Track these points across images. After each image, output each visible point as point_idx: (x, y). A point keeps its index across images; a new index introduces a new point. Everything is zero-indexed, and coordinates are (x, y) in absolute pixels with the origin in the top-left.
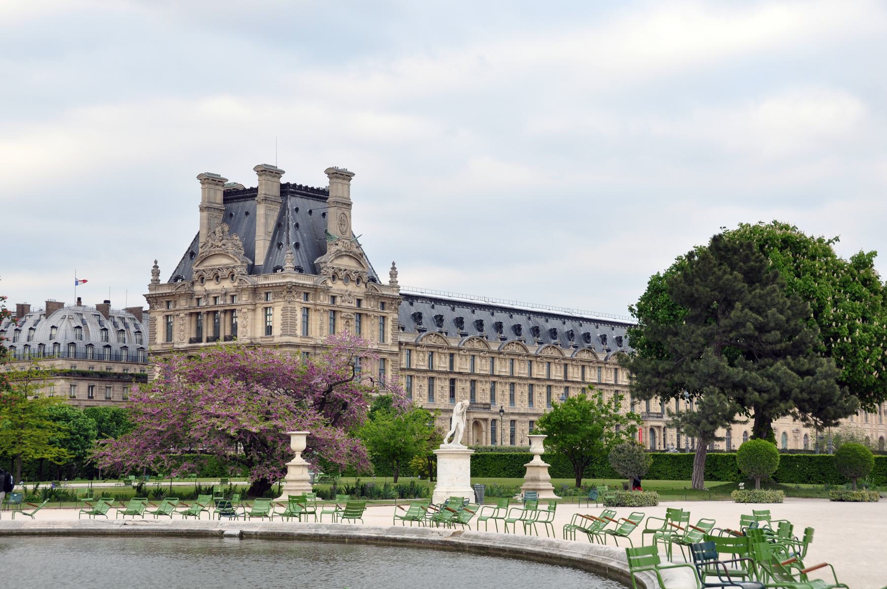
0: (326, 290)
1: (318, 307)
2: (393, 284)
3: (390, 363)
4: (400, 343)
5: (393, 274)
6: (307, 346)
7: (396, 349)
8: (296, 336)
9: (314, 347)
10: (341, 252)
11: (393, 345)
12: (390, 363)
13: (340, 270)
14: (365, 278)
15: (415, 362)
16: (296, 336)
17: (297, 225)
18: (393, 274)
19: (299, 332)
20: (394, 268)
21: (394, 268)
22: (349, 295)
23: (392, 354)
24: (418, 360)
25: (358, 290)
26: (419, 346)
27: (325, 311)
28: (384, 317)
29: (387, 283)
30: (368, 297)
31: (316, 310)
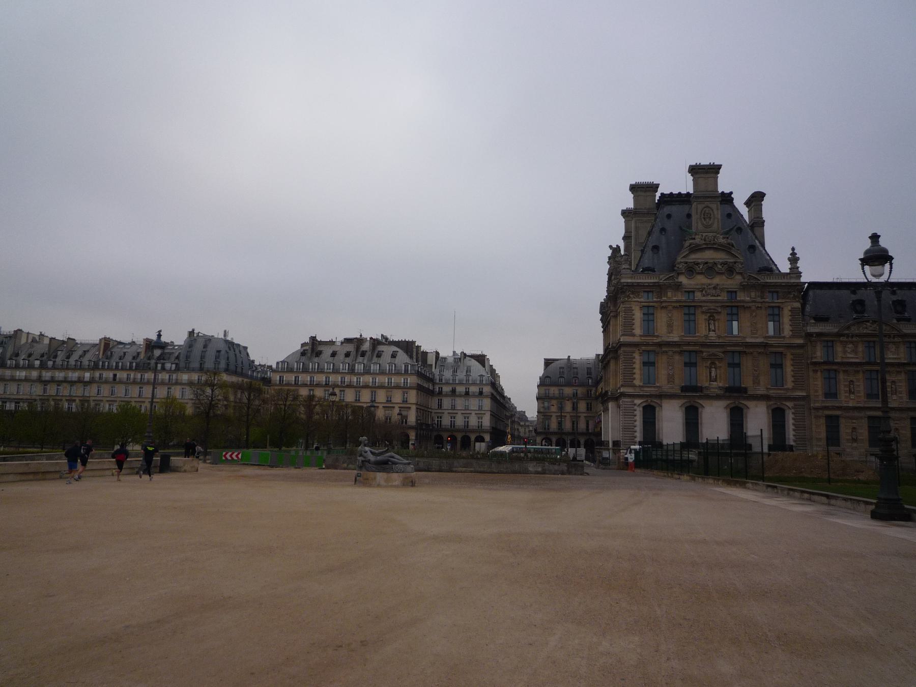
0: (678, 287)
1: (664, 304)
2: (795, 271)
3: (789, 356)
4: (809, 335)
5: (794, 259)
6: (647, 345)
7: (800, 341)
8: (634, 335)
9: (660, 345)
10: (697, 245)
11: (793, 337)
12: (789, 356)
13: (698, 264)
14: (738, 267)
15: (840, 355)
16: (634, 335)
17: (663, 230)
18: (794, 259)
19: (638, 331)
20: (793, 254)
21: (793, 254)
22: (715, 288)
23: (790, 346)
24: (845, 352)
25: (730, 282)
26: (843, 335)
27: (674, 307)
28: (779, 307)
29: (788, 271)
30: (744, 288)
31: (662, 308)
